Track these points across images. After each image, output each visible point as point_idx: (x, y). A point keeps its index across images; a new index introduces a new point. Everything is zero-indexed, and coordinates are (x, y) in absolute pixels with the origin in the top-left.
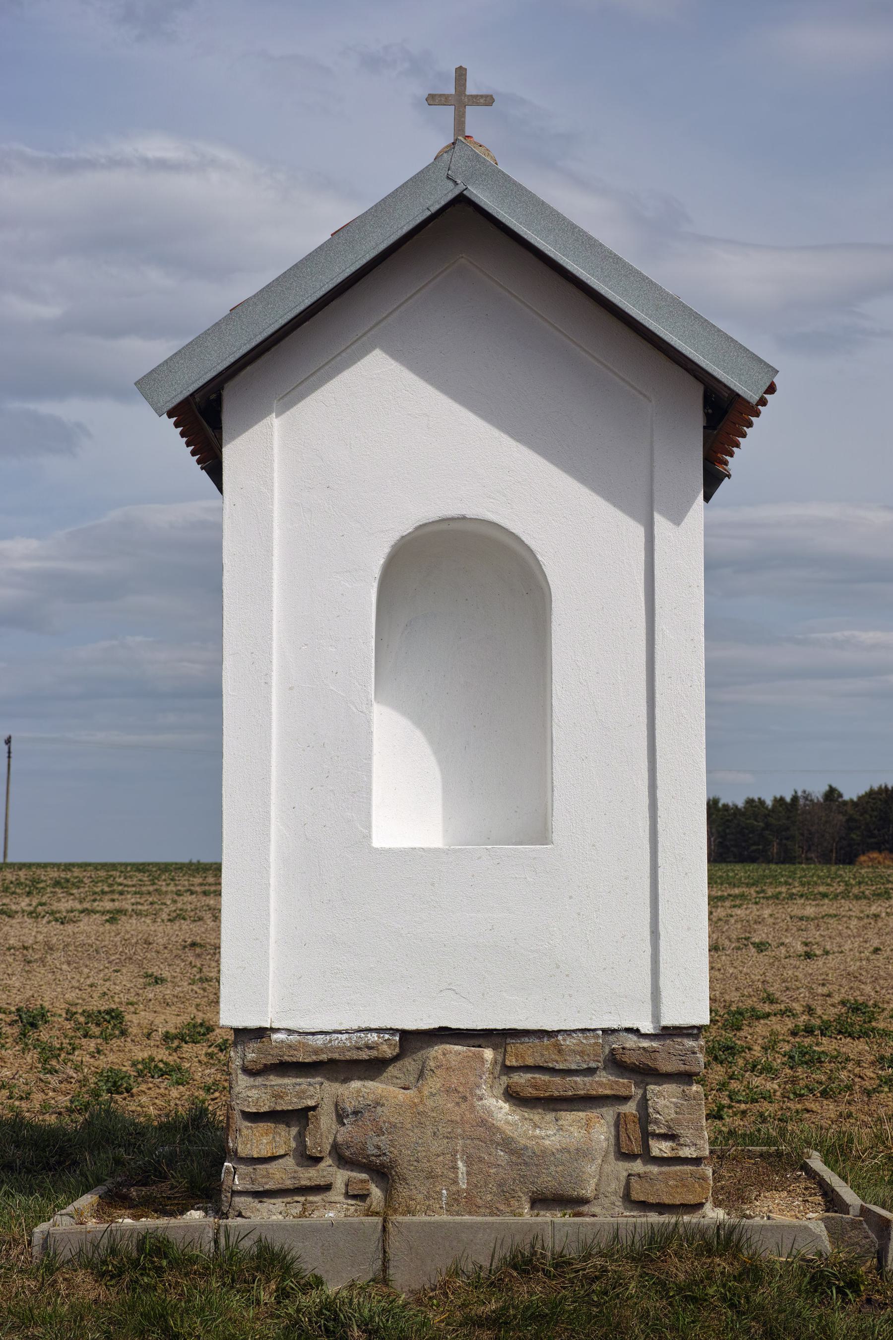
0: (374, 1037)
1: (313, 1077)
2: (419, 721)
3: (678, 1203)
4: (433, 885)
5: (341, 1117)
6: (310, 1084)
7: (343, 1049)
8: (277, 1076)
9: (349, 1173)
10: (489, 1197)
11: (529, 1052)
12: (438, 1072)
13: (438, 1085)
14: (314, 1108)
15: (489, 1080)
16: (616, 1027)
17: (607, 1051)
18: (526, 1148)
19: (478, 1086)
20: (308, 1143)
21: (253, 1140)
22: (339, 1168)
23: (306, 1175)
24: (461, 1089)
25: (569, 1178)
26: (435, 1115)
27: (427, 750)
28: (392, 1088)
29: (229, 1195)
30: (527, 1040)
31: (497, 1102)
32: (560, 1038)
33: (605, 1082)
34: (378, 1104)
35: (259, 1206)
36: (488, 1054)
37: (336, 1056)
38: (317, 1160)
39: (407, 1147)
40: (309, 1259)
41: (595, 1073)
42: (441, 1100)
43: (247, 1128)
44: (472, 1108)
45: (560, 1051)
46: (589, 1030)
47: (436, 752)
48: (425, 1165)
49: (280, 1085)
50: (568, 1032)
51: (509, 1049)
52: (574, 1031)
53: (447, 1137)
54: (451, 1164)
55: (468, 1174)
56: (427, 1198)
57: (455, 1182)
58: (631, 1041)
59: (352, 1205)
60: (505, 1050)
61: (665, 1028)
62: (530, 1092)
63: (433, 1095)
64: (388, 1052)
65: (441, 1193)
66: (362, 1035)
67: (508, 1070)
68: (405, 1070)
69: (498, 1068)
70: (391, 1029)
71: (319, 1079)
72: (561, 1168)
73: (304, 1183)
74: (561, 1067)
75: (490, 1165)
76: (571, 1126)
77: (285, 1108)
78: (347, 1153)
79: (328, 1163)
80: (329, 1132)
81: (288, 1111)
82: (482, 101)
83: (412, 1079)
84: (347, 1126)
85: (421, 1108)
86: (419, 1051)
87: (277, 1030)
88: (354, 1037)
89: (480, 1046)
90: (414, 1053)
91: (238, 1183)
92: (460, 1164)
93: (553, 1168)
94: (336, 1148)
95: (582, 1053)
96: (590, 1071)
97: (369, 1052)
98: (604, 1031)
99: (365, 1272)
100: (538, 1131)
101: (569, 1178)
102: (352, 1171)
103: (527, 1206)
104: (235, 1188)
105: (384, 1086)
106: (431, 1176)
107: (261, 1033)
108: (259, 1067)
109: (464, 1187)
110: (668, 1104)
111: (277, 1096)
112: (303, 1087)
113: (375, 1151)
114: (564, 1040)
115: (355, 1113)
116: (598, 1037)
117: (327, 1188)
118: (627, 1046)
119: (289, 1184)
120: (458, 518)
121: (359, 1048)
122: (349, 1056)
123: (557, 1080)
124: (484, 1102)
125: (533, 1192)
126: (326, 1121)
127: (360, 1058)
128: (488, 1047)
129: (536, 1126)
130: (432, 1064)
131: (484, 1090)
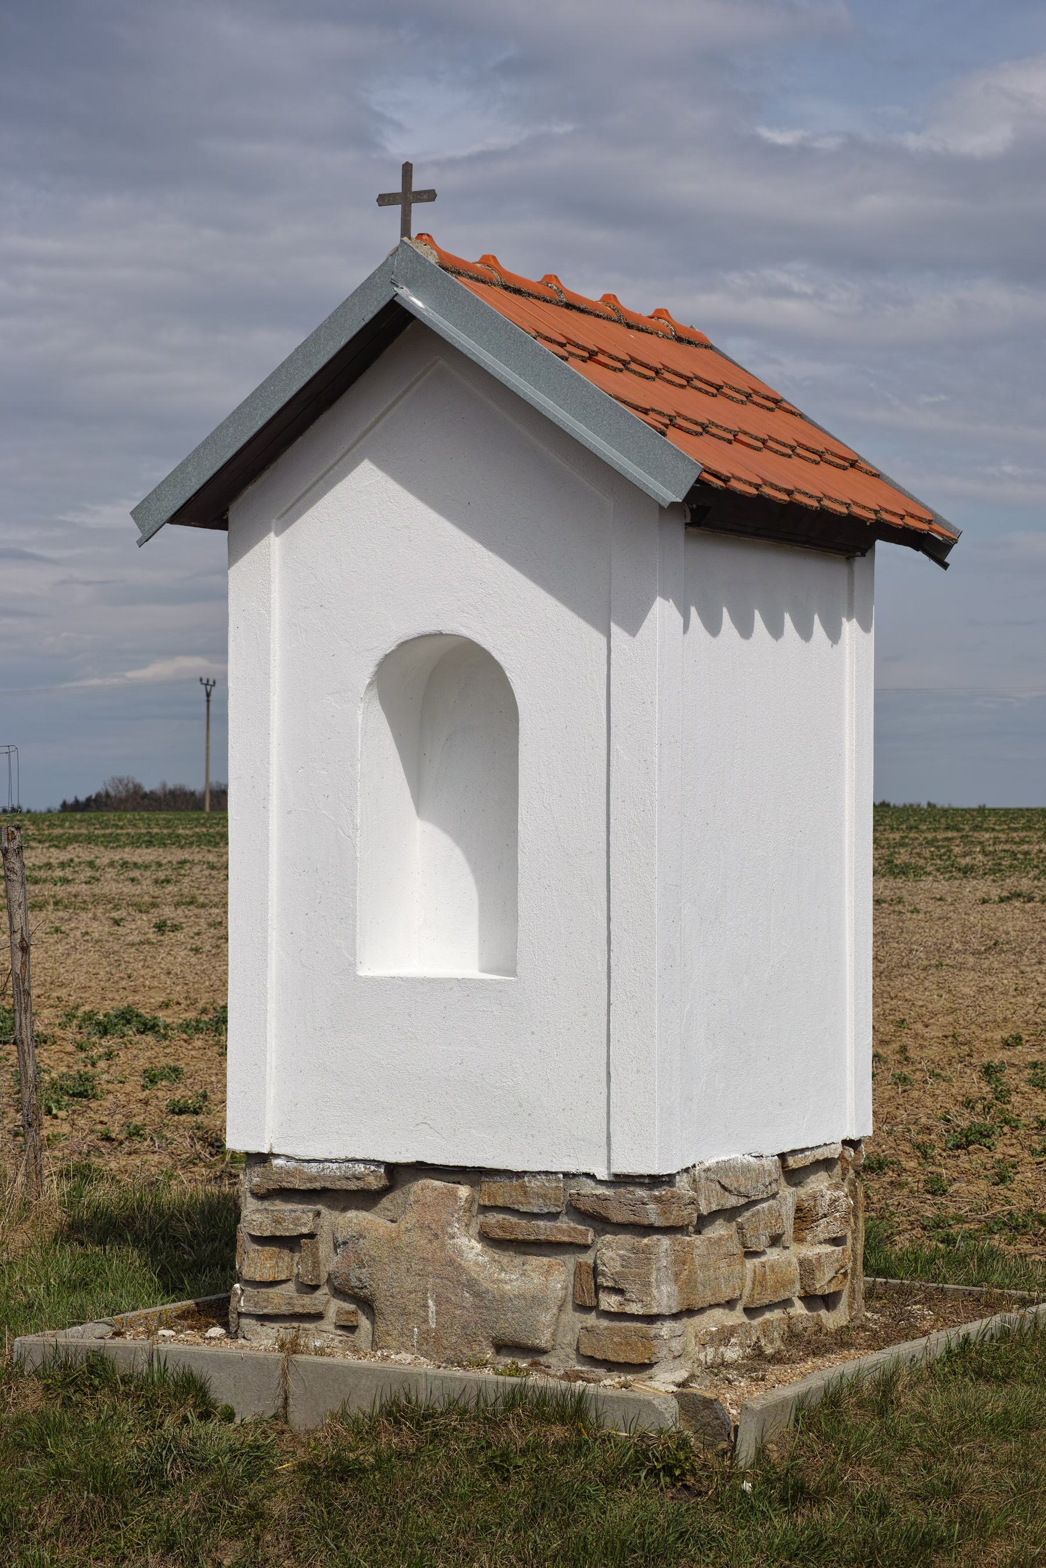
0: (360, 1168)
2: (458, 837)
3: (622, 1361)
4: (410, 1015)
7: (334, 1179)
8: (283, 1201)
9: (341, 1303)
10: (454, 1339)
13: (415, 1220)
14: (311, 1236)
16: (574, 1171)
18: (487, 1291)
21: (255, 1263)
24: (433, 1226)
25: (524, 1326)
27: (466, 869)
29: (235, 1316)
32: (526, 1179)
33: (565, 1228)
34: (361, 1236)
35: (259, 1329)
36: (464, 1191)
37: (328, 1185)
38: (316, 1288)
39: (386, 1282)
40: (223, 1391)
42: (415, 1236)
43: (254, 1251)
44: (443, 1245)
46: (552, 1173)
47: (474, 870)
49: (279, 1211)
50: (534, 1174)
52: (539, 1173)
55: (438, 1313)
56: (402, 1335)
57: (426, 1321)
58: (589, 1188)
61: (616, 1175)
62: (498, 1234)
63: (408, 1230)
64: (374, 1183)
70: (375, 1161)
71: (319, 1207)
73: (300, 1310)
75: (457, 1306)
76: (533, 1271)
77: (283, 1234)
81: (286, 1237)
82: (425, 197)
85: (397, 1243)
87: (278, 1156)
89: (459, 1183)
90: (403, 1185)
91: (243, 1306)
92: (431, 1303)
93: (509, 1315)
97: (357, 1183)
98: (566, 1175)
99: (269, 1407)
101: (524, 1326)
102: (344, 1301)
104: (239, 1310)
106: (404, 1312)
107: (261, 1159)
108: (263, 1191)
109: (433, 1326)
110: (614, 1256)
111: (277, 1222)
112: (298, 1214)
114: (530, 1182)
115: (345, 1243)
116: (559, 1180)
117: (318, 1317)
118: (582, 1192)
119: (285, 1310)
120: (435, 635)
121: (348, 1178)
122: (339, 1185)
123: (523, 1222)
124: (456, 1240)
125: (494, 1338)
127: (349, 1188)
129: (502, 1270)
131: (456, 1228)
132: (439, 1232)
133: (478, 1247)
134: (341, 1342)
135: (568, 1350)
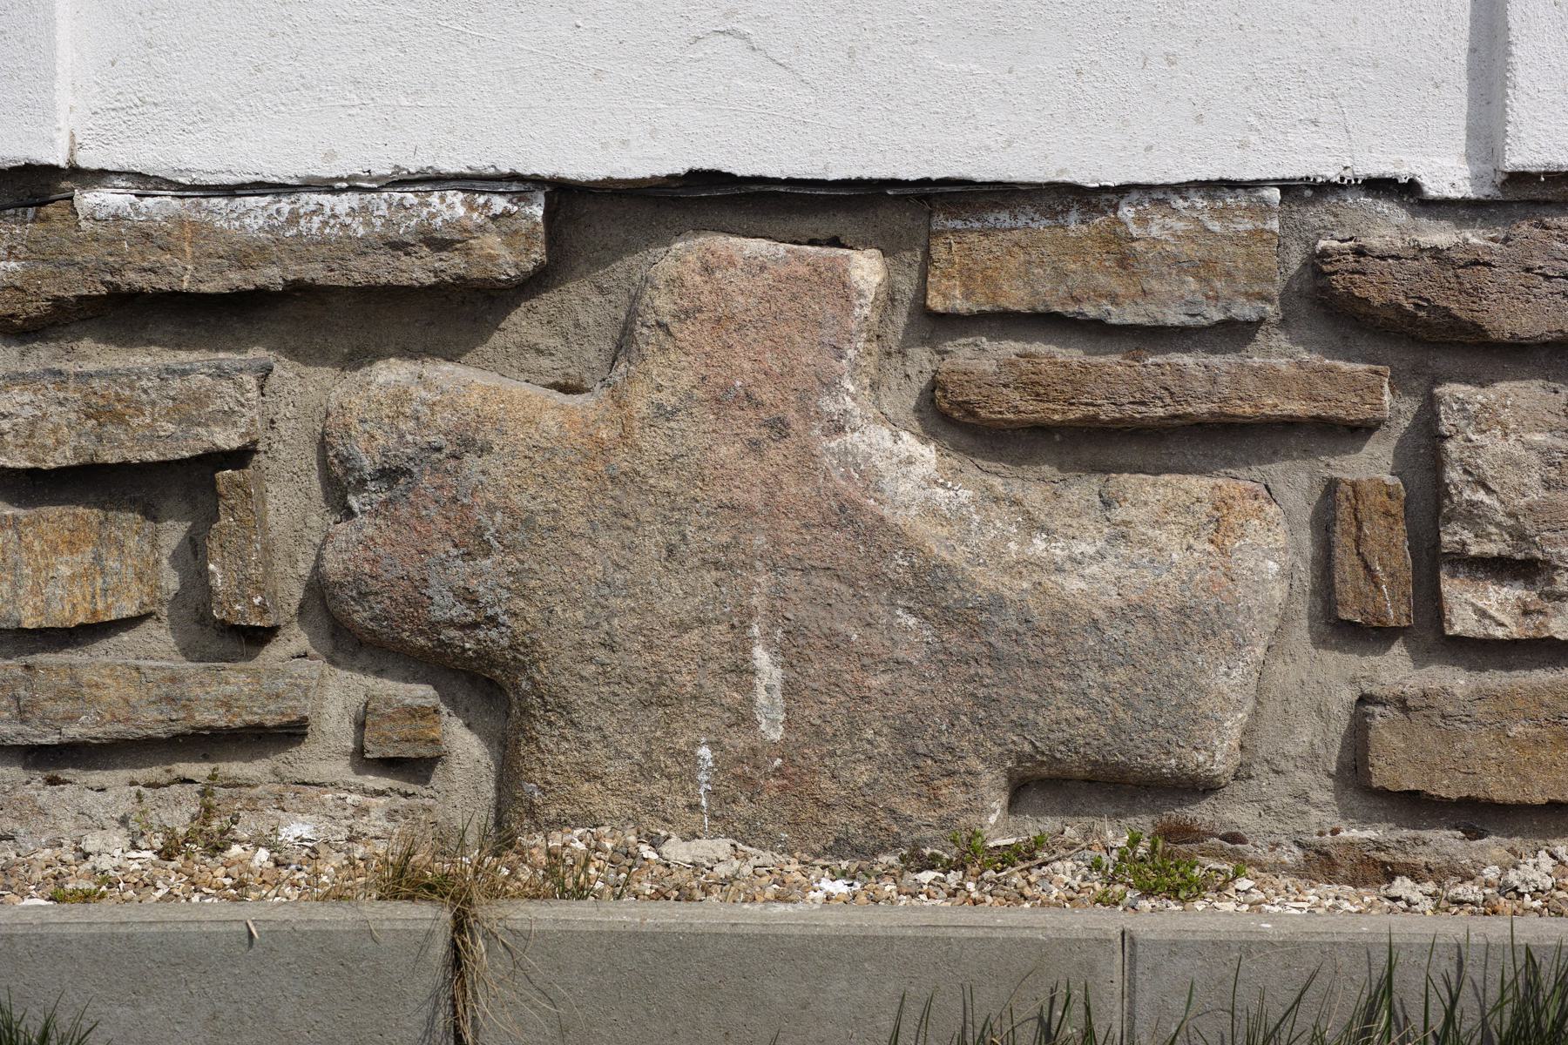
0: (451, 207)
1: (239, 345)
3: (1539, 799)
5: (337, 485)
6: (221, 373)
7: (342, 248)
8: (108, 340)
9: (370, 681)
10: (863, 774)
11: (1013, 264)
12: (684, 332)
13: (686, 380)
14: (240, 457)
15: (869, 363)
16: (1333, 175)
17: (1295, 260)
18: (998, 603)
19: (830, 385)
20: (218, 582)
22: (333, 662)
23: (216, 690)
24: (766, 394)
25: (1148, 711)
26: (671, 484)
28: (518, 388)
30: (1004, 216)
31: (896, 438)
32: (1127, 212)
33: (1284, 371)
34: (467, 444)
35: (46, 795)
36: (866, 269)
37: (315, 272)
38: (256, 637)
39: (569, 599)
41: (1251, 338)
42: (692, 432)
44: (808, 457)
45: (1125, 262)
48: (636, 660)
49: (112, 375)
51: (939, 251)
52: (1180, 189)
53: (717, 565)
54: (728, 659)
55: (791, 690)
56: (646, 772)
57: (744, 718)
59: (382, 793)
60: (927, 255)
61: (1518, 178)
62: (1016, 405)
63: (663, 413)
64: (504, 257)
65: (687, 757)
66: (410, 198)
67: (936, 325)
68: (567, 323)
69: (901, 319)
70: (514, 177)
71: (258, 354)
72: (1122, 674)
73: (208, 717)
74: (1130, 319)
75: (869, 661)
76: (1157, 524)
77: (133, 456)
78: (360, 616)
79: (294, 648)
80: (299, 540)
81: (145, 467)
83: (591, 354)
84: (361, 519)
85: (622, 460)
86: (617, 256)
87: (99, 177)
88: (381, 203)
89: (835, 242)
93: (1092, 675)
94: (321, 600)
95: (1204, 269)
96: (1234, 333)
97: (436, 261)
98: (1290, 188)
100: (1039, 544)
101: (1148, 711)
102: (380, 673)
103: (997, 803)
105: (492, 380)
106: (658, 697)
108: (35, 307)
109: (776, 735)
110: (1518, 451)
111: (102, 414)
112: (195, 381)
113: (458, 611)
114: (1143, 221)
115: (389, 475)
116: (1265, 209)
117: (292, 733)
118: (1374, 242)
119: (152, 721)
121: (398, 246)
122: (361, 271)
123: (1112, 361)
124: (851, 438)
125: (1020, 758)
126: (285, 499)
127: (404, 280)
128: (867, 244)
129: (1032, 525)
130: (663, 303)
131: (850, 398)
132: (791, 415)
133: (927, 455)
134: (391, 815)
135: (1303, 778)
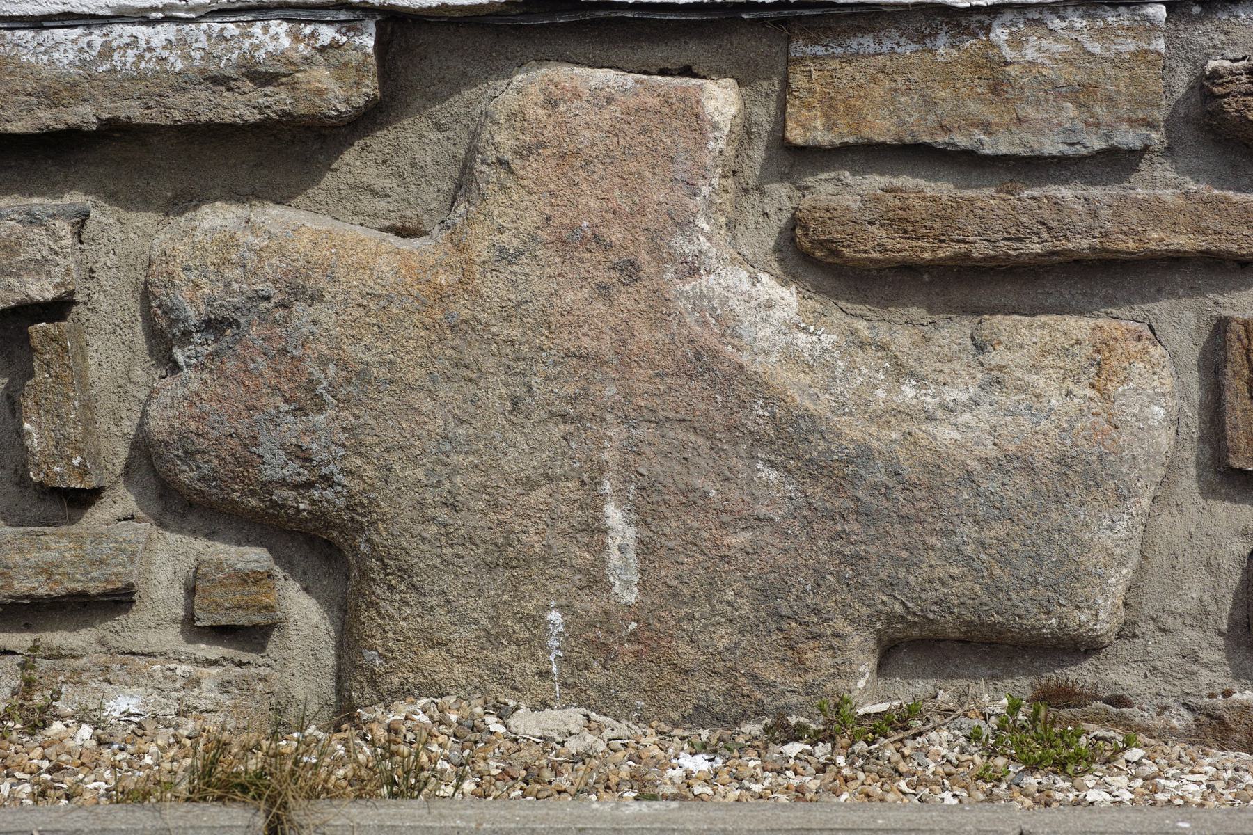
1: (55, 189)
5: (163, 337)
6: (32, 219)
9: (200, 544)
10: (723, 638)
11: (878, 92)
12: (527, 169)
13: (530, 221)
14: (58, 309)
15: (725, 201)
17: (1182, 83)
18: (865, 454)
19: (684, 224)
20: (34, 442)
22: (162, 525)
23: (36, 556)
24: (615, 234)
25: (1027, 568)
26: (515, 332)
28: (351, 232)
30: (868, 41)
31: (755, 280)
32: (1000, 34)
36: (721, 99)
37: (131, 110)
38: (79, 500)
41: (1134, 168)
42: (535, 275)
44: (660, 302)
45: (998, 88)
48: (480, 520)
51: (798, 80)
53: (565, 418)
54: (578, 517)
55: (645, 549)
56: (493, 638)
57: (596, 581)
59: (214, 663)
60: (785, 83)
63: (506, 257)
64: (333, 92)
65: (537, 622)
66: (231, 29)
67: (795, 158)
68: (403, 162)
69: (758, 153)
71: (75, 199)
72: (998, 529)
74: (1004, 149)
75: (728, 518)
76: (1034, 368)
78: (187, 476)
79: (120, 510)
80: (123, 396)
83: (428, 194)
84: (187, 373)
85: (462, 308)
86: (455, 90)
88: (200, 34)
89: (687, 72)
92: (614, 515)
93: (967, 530)
94: (146, 455)
95: (1083, 94)
96: (1116, 163)
100: (908, 391)
101: (1027, 568)
102: (211, 536)
103: (866, 666)
105: (323, 223)
106: (504, 559)
109: (631, 598)
113: (290, 470)
114: (1016, 43)
115: (215, 326)
116: (1150, 27)
117: (118, 601)
121: (219, 81)
123: (985, 195)
124: (707, 281)
125: (891, 619)
126: (107, 351)
127: (227, 117)
128: (721, 74)
129: (901, 371)
130: (504, 139)
131: (706, 237)
132: (643, 257)
133: (788, 298)
134: (224, 686)
135: (1191, 636)
